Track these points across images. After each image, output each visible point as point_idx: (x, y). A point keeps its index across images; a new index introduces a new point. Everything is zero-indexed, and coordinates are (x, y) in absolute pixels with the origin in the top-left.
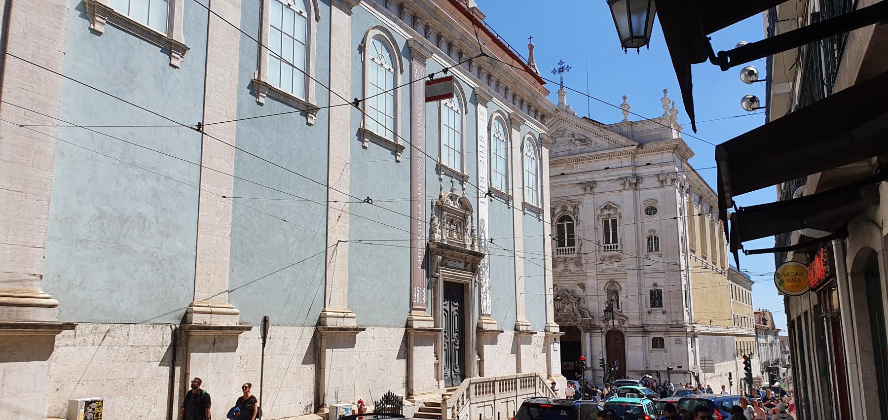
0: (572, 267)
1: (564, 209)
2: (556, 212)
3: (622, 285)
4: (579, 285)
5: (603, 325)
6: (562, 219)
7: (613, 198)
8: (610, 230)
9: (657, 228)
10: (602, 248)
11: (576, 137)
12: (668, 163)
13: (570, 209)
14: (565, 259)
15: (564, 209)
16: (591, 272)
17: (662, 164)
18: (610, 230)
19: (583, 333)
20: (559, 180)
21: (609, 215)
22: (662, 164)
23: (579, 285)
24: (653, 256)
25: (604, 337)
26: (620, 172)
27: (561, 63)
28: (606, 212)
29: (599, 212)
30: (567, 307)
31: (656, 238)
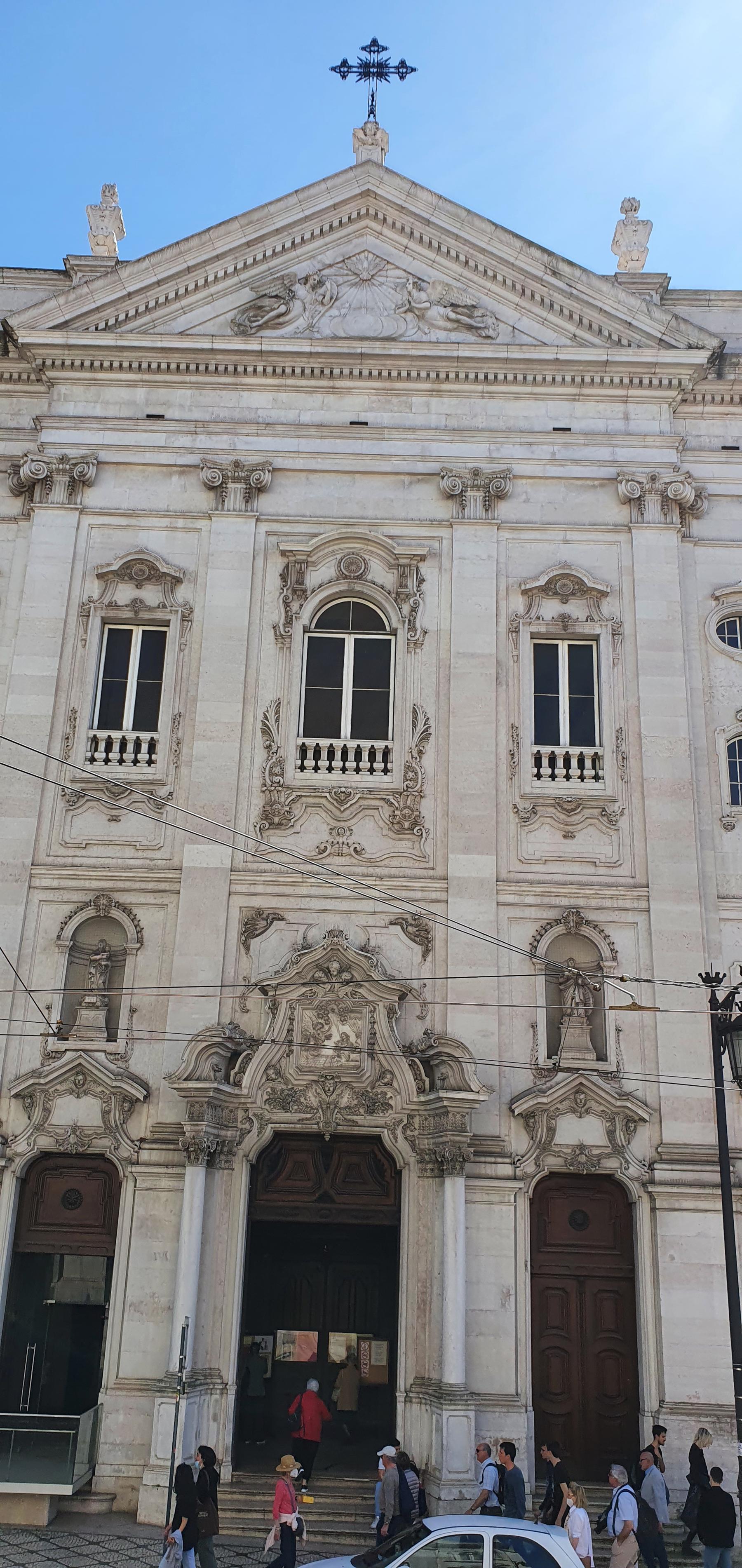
0: (369, 832)
1: (353, 569)
2: (313, 578)
3: (623, 939)
5: (517, 1140)
6: (334, 617)
7: (591, 557)
8: (565, 692)
13: (380, 573)
14: (341, 797)
15: (353, 569)
16: (470, 866)
18: (565, 692)
19: (414, 1188)
20: (341, 445)
21: (564, 620)
25: (524, 1206)
26: (623, 454)
27: (374, 46)
28: (550, 608)
29: (518, 603)
30: (338, 1030)
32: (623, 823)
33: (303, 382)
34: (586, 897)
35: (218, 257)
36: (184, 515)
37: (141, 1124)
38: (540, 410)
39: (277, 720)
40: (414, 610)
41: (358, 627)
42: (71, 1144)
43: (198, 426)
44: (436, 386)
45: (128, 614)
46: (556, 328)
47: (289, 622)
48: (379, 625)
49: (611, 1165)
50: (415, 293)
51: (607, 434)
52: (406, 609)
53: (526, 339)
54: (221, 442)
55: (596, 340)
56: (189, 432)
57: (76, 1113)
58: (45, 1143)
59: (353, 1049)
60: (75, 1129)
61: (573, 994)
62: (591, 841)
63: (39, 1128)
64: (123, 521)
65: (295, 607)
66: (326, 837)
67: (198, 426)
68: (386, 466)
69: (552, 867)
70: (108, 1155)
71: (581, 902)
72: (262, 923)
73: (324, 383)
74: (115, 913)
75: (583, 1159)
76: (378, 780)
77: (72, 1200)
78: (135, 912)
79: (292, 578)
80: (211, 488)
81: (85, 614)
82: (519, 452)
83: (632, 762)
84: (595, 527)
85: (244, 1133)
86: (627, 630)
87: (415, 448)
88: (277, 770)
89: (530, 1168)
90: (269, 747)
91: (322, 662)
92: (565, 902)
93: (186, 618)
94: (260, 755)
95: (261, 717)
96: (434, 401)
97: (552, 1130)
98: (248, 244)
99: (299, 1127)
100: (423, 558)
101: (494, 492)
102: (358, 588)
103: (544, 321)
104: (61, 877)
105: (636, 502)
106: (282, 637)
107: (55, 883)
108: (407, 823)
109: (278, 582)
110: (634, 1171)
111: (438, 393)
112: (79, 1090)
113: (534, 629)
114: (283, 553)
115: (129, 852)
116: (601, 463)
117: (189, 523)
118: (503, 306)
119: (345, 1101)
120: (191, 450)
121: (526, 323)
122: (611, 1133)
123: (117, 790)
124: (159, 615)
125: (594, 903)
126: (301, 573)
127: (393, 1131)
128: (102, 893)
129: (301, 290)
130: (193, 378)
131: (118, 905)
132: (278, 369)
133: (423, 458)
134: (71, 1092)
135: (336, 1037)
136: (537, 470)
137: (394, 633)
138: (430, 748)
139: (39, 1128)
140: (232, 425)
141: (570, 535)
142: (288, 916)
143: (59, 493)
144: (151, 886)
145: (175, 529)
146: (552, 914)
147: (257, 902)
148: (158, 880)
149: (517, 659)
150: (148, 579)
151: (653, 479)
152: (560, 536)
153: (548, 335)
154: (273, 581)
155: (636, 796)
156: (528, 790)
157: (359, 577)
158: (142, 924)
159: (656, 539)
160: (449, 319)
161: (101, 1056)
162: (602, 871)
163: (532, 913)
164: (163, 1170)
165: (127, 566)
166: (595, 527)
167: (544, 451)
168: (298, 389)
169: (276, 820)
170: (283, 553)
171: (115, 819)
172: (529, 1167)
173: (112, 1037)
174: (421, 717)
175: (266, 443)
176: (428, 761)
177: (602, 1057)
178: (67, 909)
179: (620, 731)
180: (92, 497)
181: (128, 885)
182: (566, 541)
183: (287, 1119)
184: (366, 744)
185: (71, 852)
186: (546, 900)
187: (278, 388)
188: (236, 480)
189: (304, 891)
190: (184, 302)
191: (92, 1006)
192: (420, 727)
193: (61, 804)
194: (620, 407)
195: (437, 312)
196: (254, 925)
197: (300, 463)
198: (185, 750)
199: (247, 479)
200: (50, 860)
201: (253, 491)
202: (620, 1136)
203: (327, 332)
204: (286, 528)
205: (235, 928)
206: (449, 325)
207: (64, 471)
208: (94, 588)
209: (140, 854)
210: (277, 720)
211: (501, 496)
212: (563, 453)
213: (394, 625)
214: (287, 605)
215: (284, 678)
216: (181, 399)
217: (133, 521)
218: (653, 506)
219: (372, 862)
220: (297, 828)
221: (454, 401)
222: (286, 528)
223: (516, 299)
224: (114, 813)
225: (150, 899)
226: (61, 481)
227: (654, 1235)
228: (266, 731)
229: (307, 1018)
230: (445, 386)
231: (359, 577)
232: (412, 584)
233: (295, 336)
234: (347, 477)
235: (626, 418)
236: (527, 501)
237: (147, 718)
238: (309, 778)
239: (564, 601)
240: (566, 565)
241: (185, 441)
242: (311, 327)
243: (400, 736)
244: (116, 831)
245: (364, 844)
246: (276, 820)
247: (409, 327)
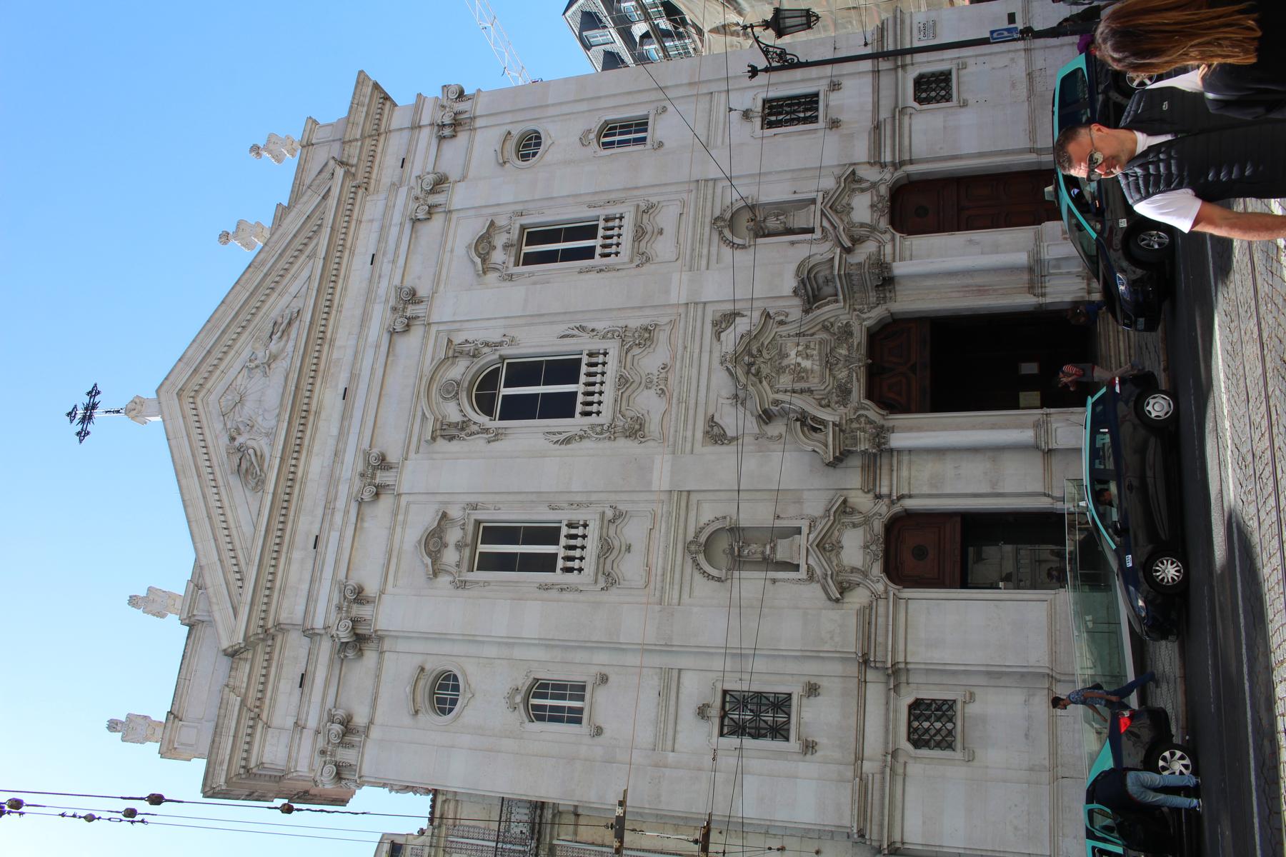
0: (650, 362)
1: (451, 390)
2: (455, 417)
4: (718, 335)
5: (869, 248)
7: (466, 231)
8: (558, 243)
9: (578, 127)
14: (623, 382)
15: (451, 390)
16: (679, 289)
18: (558, 243)
23: (718, 335)
28: (498, 256)
29: (492, 276)
30: (793, 358)
31: (609, 129)
32: (654, 200)
33: (308, 433)
34: (704, 216)
35: (204, 497)
36: (395, 514)
37: (862, 501)
38: (358, 269)
39: (560, 433)
40: (487, 344)
41: (494, 386)
42: (878, 549)
43: (329, 507)
44: (328, 341)
45: (467, 552)
46: (301, 269)
47: (487, 431)
48: (496, 372)
49: (883, 190)
50: (257, 362)
51: (382, 228)
52: (486, 350)
53: (304, 289)
54: (343, 490)
55: (315, 242)
56: (333, 514)
57: (855, 548)
58: (877, 569)
59: (807, 347)
60: (866, 547)
61: (772, 223)
62: (666, 218)
63: (865, 574)
64: (394, 561)
65: (474, 428)
66: (652, 391)
67: (329, 507)
70: (885, 520)
71: (708, 220)
72: (715, 429)
73: (311, 418)
74: (703, 539)
75: (880, 205)
76: (612, 361)
77: (920, 553)
78: (701, 524)
79: (454, 432)
80: (377, 494)
81: (463, 585)
82: (384, 283)
83: (613, 196)
84: (445, 233)
85: (870, 422)
86: (519, 208)
87: (370, 354)
88: (598, 429)
89: (887, 237)
90: (581, 438)
91: (518, 409)
92: (707, 229)
93: (475, 507)
94: (586, 444)
95: (557, 446)
96: (338, 343)
97: (862, 225)
98: (199, 476)
99: (863, 380)
100: (450, 341)
101: (412, 297)
102: (466, 384)
103: (295, 277)
104: (672, 583)
105: (431, 210)
106: (497, 436)
107: (677, 587)
108: (646, 336)
109: (454, 442)
110: (888, 176)
111: (332, 341)
112: (837, 547)
113: (511, 264)
114: (434, 439)
115: (655, 534)
116: (401, 232)
117: (402, 511)
118: (277, 306)
119: (844, 352)
120: (347, 512)
121: (293, 289)
122: (863, 190)
123: (606, 548)
124: (470, 528)
126: (449, 425)
127: (864, 320)
128: (687, 547)
129: (240, 440)
130: (292, 513)
131: (696, 536)
132: (295, 449)
133: (378, 346)
134: (838, 554)
135: (799, 360)
136: (399, 272)
137: (503, 358)
138: (590, 325)
139: (865, 574)
140: (332, 481)
141: (448, 248)
142: (710, 414)
143: (364, 611)
144: (683, 513)
145: (405, 522)
146: (716, 237)
147: (699, 435)
148: (679, 507)
149: (532, 274)
150: (441, 538)
151: (417, 198)
152: (447, 255)
153: (305, 274)
154: (455, 446)
155: (635, 193)
156: (626, 259)
157: (458, 384)
158: (712, 518)
159: (459, 197)
160: (281, 337)
161: (812, 537)
163: (714, 249)
164: (895, 474)
165: (429, 554)
166: (445, 233)
167: (386, 268)
168: (313, 438)
169: (637, 427)
170: (434, 439)
171: (629, 549)
172: (887, 237)
173: (798, 531)
174: (571, 332)
175: (349, 457)
176: (601, 326)
177: (813, 201)
178: (698, 577)
179: (589, 207)
180: (371, 589)
181: (681, 531)
182: (452, 251)
183: (858, 390)
184: (584, 369)
185: (652, 579)
186: (706, 241)
187: (309, 452)
188: (373, 476)
189: (692, 402)
190: (232, 525)
191: (773, 549)
192: (576, 332)
193: (614, 590)
194: (363, 226)
195: (274, 347)
196: (716, 435)
197: (368, 433)
198: (578, 498)
199: (375, 468)
200: (658, 594)
201: (383, 463)
202: (864, 185)
203: (273, 422)
204: (415, 439)
205: (718, 448)
206: (285, 338)
207: (348, 607)
208: (444, 579)
209: (657, 526)
210: (560, 433)
211: (413, 293)
212: (390, 256)
213: (496, 356)
214: (473, 434)
215: (529, 434)
216: (306, 524)
217: (395, 554)
218: (434, 199)
219: (674, 358)
220: (645, 412)
221: (340, 330)
222: (415, 439)
223: (275, 295)
224: (623, 548)
225: (692, 514)
226: (357, 611)
227: (927, 161)
228: (568, 441)
229: (785, 381)
230: (329, 335)
231: (458, 384)
232: (467, 347)
233: (272, 445)
234: (383, 399)
235: (372, 221)
236: (419, 278)
237: (549, 535)
238: (607, 409)
239: (495, 248)
240: (469, 247)
241: (338, 518)
242: (267, 435)
243: (580, 346)
244: (639, 547)
245: (660, 364)
246: (637, 427)
247: (280, 367)
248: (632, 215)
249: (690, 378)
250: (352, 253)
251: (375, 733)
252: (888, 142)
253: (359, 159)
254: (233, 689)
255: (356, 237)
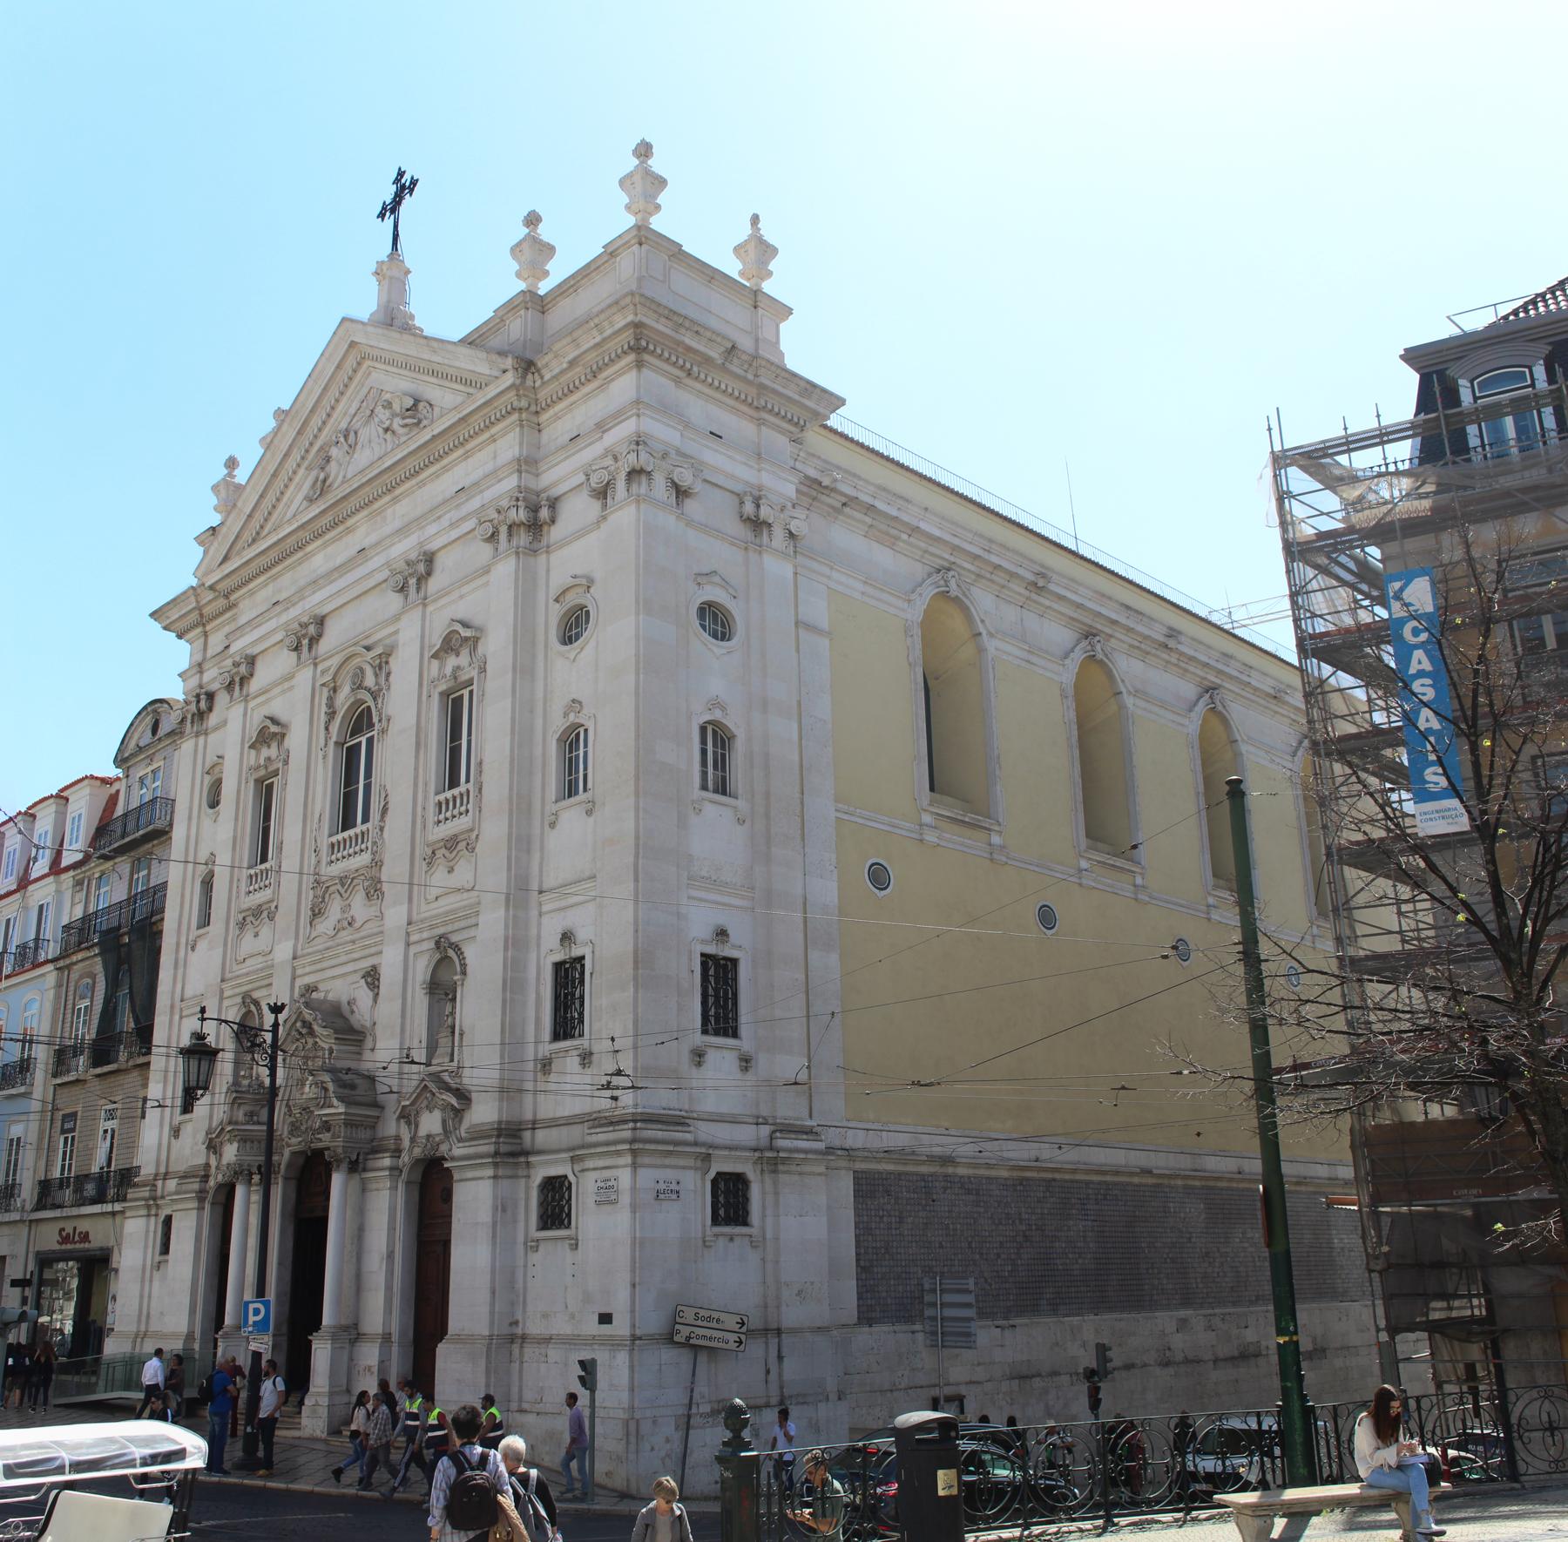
0: (359, 907)
10: (431, 809)
11: (396, 407)
12: (618, 416)
17: (602, 427)
22: (602, 427)
24: (572, 816)
34: (445, 923)
68: (372, 583)
69: (441, 902)
71: (450, 928)
98: (299, 433)
122: (444, 1122)
125: (457, 926)
129: (334, 452)
138: (387, 819)
162: (465, 895)
168: (334, 540)
187: (325, 545)
189: (325, 965)
248: (465, 827)
249: (337, 956)
250: (467, 456)
251: (201, 739)
252: (471, 1151)
253: (555, 377)
254: (197, 596)
255: (481, 447)
